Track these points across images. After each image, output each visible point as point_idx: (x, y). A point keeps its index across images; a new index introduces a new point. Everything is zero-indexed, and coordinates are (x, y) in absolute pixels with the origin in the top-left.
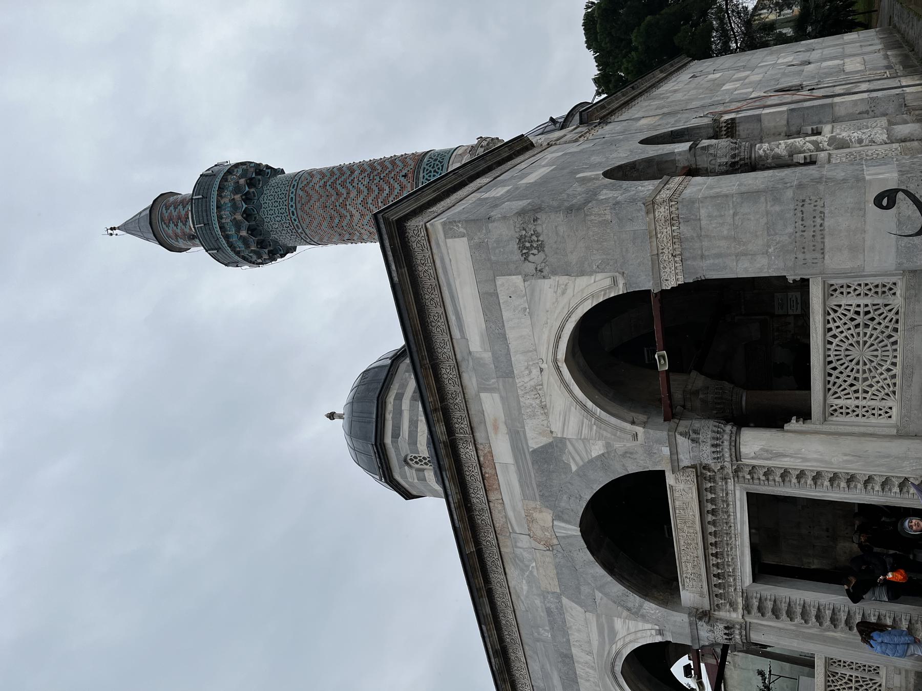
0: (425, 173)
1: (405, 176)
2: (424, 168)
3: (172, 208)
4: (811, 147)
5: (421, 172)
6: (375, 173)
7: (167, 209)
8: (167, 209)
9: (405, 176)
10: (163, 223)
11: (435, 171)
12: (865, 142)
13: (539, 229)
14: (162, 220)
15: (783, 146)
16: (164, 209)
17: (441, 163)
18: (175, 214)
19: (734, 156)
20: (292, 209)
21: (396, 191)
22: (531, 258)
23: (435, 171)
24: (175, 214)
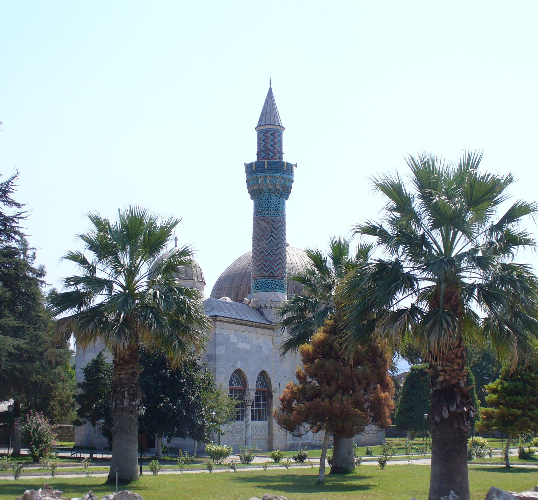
0: (272, 281)
1: (271, 272)
2: (274, 281)
3: (272, 137)
4: (247, 419)
5: (272, 280)
6: (274, 257)
7: (271, 134)
8: (271, 134)
9: (271, 272)
10: (265, 132)
11: (272, 286)
12: (246, 432)
13: (213, 361)
14: (267, 131)
15: (248, 413)
16: (272, 132)
17: (275, 288)
18: (269, 140)
19: (246, 401)
20: (263, 214)
21: (265, 268)
22: (207, 358)
23: (272, 286)
24: (269, 140)
